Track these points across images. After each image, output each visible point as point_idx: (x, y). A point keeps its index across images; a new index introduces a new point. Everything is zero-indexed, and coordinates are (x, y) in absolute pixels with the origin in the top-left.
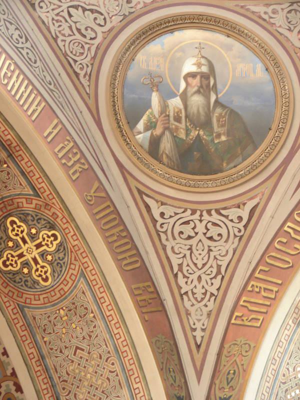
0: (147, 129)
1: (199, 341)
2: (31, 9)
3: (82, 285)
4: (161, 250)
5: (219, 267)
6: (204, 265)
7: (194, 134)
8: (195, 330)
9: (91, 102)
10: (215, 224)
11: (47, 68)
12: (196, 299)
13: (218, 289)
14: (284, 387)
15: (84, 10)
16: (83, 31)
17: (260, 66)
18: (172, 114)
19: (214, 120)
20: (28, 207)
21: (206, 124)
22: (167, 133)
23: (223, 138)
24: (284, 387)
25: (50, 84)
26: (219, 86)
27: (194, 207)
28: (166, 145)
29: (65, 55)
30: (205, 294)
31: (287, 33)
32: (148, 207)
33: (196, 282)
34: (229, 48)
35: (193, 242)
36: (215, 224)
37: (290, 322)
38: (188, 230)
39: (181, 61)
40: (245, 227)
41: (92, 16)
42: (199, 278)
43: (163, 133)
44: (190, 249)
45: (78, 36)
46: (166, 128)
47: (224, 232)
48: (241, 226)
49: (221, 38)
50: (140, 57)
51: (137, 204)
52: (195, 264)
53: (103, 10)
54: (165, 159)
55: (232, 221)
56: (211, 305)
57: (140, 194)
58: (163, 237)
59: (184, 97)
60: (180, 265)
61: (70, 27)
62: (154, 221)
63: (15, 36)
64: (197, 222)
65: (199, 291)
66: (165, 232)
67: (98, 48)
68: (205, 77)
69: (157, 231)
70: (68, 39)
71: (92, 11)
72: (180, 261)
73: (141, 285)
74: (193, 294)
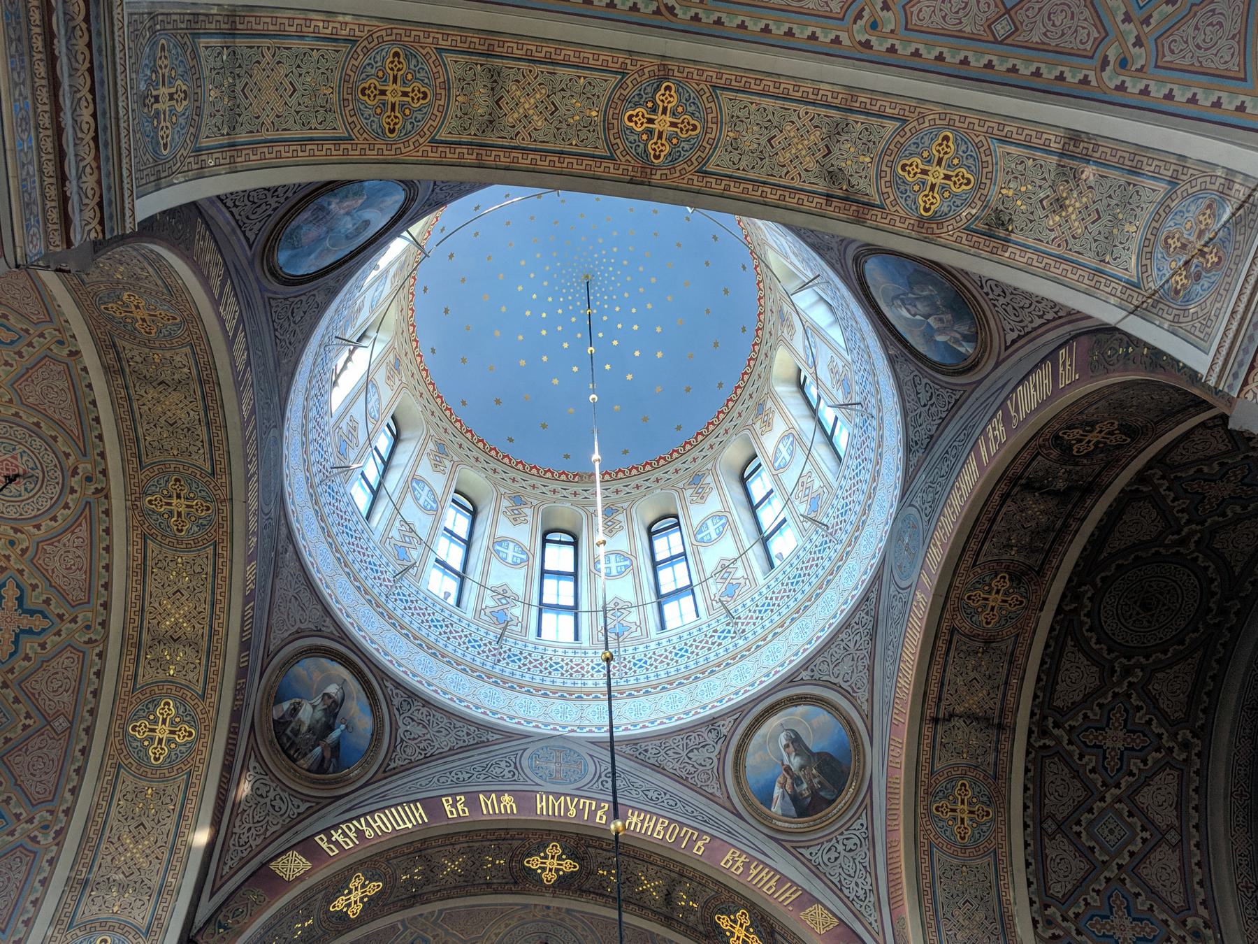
0: (961, 345)
3: (1092, 410)
14: (1071, 241)
15: (918, 393)
16: (929, 394)
24: (1071, 241)
29: (949, 411)
32: (1014, 342)
37: (1007, 255)
38: (1009, 309)
39: (906, 319)
41: (918, 387)
59: (927, 316)
61: (932, 405)
73: (1061, 369)
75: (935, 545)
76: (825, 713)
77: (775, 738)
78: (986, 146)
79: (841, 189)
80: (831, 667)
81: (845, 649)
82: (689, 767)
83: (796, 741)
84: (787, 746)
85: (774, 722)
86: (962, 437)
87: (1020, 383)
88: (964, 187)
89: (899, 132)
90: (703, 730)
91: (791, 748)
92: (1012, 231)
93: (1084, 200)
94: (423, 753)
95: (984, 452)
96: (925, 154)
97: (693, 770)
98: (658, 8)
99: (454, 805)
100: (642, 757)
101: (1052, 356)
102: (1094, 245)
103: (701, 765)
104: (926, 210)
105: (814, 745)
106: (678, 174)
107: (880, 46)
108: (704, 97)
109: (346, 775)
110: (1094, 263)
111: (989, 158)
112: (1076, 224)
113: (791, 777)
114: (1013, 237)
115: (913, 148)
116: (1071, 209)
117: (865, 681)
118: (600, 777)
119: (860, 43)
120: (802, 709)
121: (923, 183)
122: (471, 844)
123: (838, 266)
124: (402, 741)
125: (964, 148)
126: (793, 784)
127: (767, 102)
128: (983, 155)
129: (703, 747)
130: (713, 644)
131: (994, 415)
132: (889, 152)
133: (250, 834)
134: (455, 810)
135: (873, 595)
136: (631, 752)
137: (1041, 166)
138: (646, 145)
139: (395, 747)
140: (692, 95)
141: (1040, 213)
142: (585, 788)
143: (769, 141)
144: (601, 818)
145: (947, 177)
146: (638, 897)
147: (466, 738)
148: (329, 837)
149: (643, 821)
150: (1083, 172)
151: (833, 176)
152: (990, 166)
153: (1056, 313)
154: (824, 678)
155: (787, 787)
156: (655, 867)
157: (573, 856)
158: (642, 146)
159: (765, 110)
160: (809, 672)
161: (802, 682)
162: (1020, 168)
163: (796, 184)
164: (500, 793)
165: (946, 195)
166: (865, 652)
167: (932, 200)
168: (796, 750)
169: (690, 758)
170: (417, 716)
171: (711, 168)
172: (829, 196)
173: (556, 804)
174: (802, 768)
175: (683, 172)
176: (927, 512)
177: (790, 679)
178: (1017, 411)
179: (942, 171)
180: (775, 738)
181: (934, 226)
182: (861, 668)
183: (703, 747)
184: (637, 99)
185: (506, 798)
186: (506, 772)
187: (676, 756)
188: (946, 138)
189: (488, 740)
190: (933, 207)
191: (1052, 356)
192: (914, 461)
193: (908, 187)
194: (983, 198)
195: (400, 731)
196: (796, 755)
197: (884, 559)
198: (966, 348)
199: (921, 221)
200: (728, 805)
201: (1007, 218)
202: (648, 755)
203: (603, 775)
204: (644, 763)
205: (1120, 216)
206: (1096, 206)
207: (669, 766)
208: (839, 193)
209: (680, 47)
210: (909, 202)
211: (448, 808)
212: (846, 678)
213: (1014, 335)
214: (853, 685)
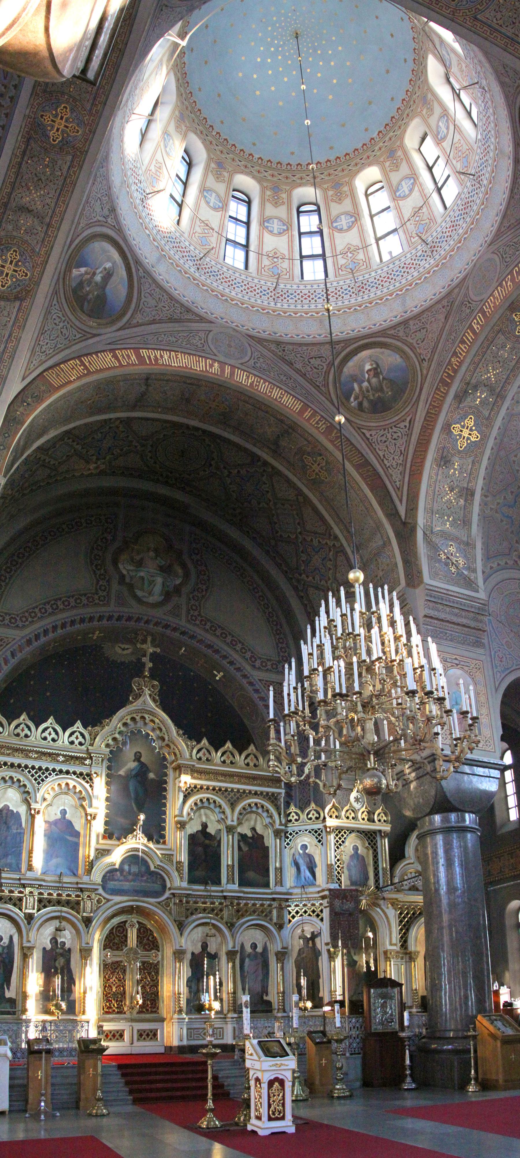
9: (328, 396)
11: (303, 387)
20: (309, 450)
34: (383, 353)
45: (315, 370)
50: (345, 370)
63: (284, 379)
75: (248, 378)
117: (147, 319)
123: (392, 332)
135: (190, 316)
156: (53, 205)
197: (211, 322)
213: (368, 436)
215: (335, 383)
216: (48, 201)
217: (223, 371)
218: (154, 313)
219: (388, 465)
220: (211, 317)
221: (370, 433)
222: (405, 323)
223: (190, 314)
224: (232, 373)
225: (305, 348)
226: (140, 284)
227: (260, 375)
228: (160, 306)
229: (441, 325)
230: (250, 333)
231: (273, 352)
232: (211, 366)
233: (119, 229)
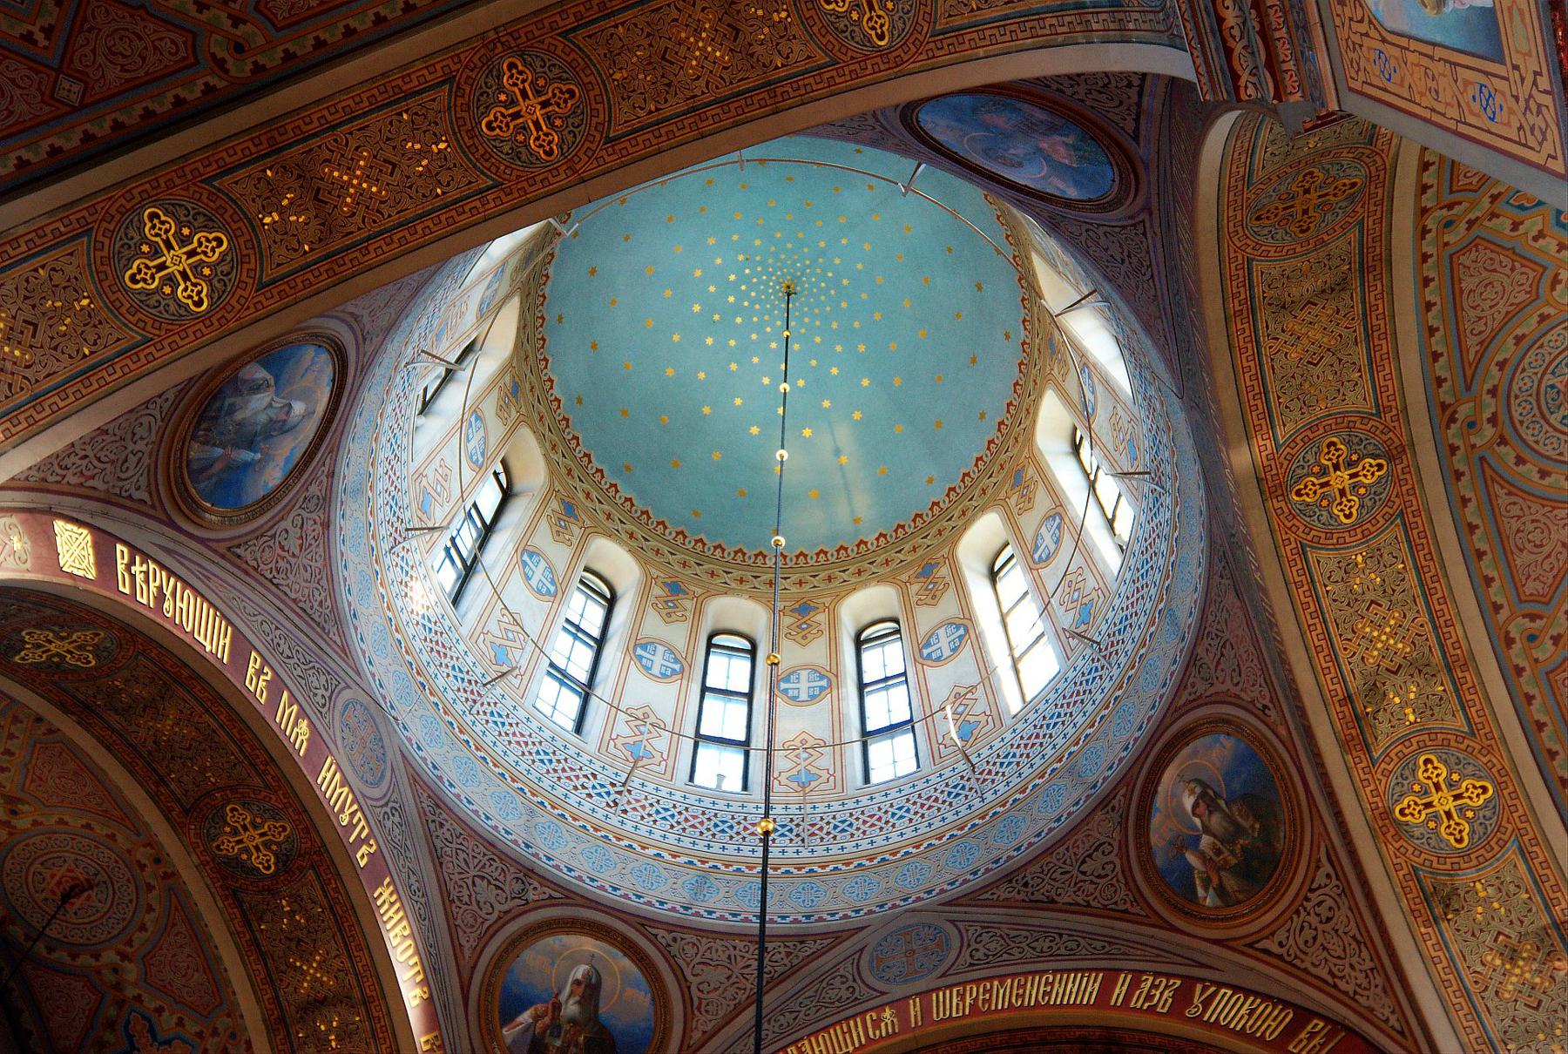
0: (1206, 889)
1: (1397, 1026)
2: (1051, 906)
4: (1306, 976)
5: (1354, 937)
6: (1344, 950)
7: (1238, 849)
8: (1387, 1021)
9: (1153, 920)
10: (1320, 904)
12: (1365, 989)
13: (1372, 960)
14: (1490, 993)
16: (1103, 873)
17: (1222, 738)
18: (1211, 854)
19: (1240, 820)
21: (1239, 831)
22: (1223, 873)
23: (1257, 826)
25: (1104, 947)
26: (1217, 789)
27: (1293, 908)
28: (1231, 883)
29: (1105, 907)
30: (1367, 976)
31: (1213, 690)
32: (1266, 951)
33: (1353, 974)
35: (1320, 939)
36: (1320, 904)
37: (1423, 930)
38: (1308, 933)
39: (1181, 806)
40: (1338, 879)
42: (1352, 966)
43: (1220, 878)
44: (1324, 949)
46: (1218, 870)
47: (1330, 902)
48: (1334, 882)
49: (1186, 751)
50: (1154, 839)
51: (1257, 959)
52: (1339, 957)
53: (1103, 839)
54: (1241, 897)
55: (1326, 885)
56: (1379, 980)
57: (1250, 946)
58: (1296, 962)
59: (1207, 830)
60: (1331, 972)
62: (1280, 957)
64: (1308, 918)
65: (1361, 979)
66: (1296, 957)
67: (1123, 872)
68: (1203, 795)
69: (1289, 963)
70: (1097, 894)
71: (1096, 850)
72: (1327, 970)
73: (1303, 1035)
74: (1360, 986)
75: (962, 996)
76: (649, 995)
77: (574, 961)
78: (1505, 837)
79: (1365, 708)
80: (698, 959)
81: (729, 957)
82: (465, 892)
83: (590, 990)
84: (577, 983)
85: (588, 944)
86: (1099, 945)
87: (1236, 989)
88: (1452, 839)
89: (1460, 737)
90: (512, 870)
91: (581, 989)
92: (1449, 920)
93: (1537, 980)
94: (274, 572)
95: (1120, 991)
96: (1455, 777)
97: (466, 899)
98: (1450, 405)
99: (259, 672)
100: (432, 826)
101: (1303, 1015)
102: (1508, 1022)
103: (478, 902)
104: (1402, 812)
105: (606, 1008)
106: (1289, 525)
107: (1517, 655)
108: (1387, 509)
109: (205, 510)
110: (1496, 1037)
111: (1497, 848)
112: (1510, 987)
113: (553, 1019)
114: (1444, 925)
115: (1453, 760)
116: (1517, 971)
117: (721, 1013)
118: (387, 804)
119: (1508, 633)
120: (626, 963)
121: (1426, 793)
122: (221, 732)
124: (273, 536)
125: (1488, 814)
126: (547, 1027)
127: (1412, 576)
128: (1495, 840)
129: (497, 887)
130: (584, 787)
131: (1168, 976)
132: (1433, 736)
133: (79, 462)
134: (256, 683)
135: (811, 947)
136: (427, 809)
137: (1530, 911)
138: (1308, 475)
139: (262, 536)
140: (1383, 496)
141: (1488, 939)
142: (369, 802)
143: (1372, 602)
144: (363, 856)
145: (1448, 814)
146: (283, 968)
147: (316, 605)
148: (132, 562)
149: (392, 904)
150: (1559, 960)
151: (1374, 690)
152: (1491, 854)
153: (1355, 993)
154: (681, 962)
155: (540, 1024)
156: (348, 964)
157: (284, 859)
158: (1305, 471)
159: (1403, 580)
160: (669, 937)
161: (652, 938)
162: (1512, 888)
163: (1342, 655)
164: (302, 714)
165: (1432, 825)
166: (749, 986)
167: (1416, 813)
168: (583, 997)
169: (474, 884)
170: (309, 526)
171: (1312, 557)
172: (1349, 698)
173: (338, 791)
174: (572, 1021)
175: (1294, 529)
176: (977, 955)
177: (644, 923)
178: (1206, 1003)
179: (1451, 805)
180: (574, 961)
181: (1392, 831)
182: (728, 994)
183: (497, 887)
184: (1356, 440)
185: (304, 724)
186: (320, 692)
187: (463, 865)
188: (1485, 789)
189: (328, 634)
190: (1409, 818)
191: (1303, 1015)
192: (1003, 892)
193: (1411, 779)
194: (1456, 866)
195: (283, 525)
196: (579, 1002)
197: (863, 928)
198: (1209, 899)
199: (1387, 814)
200: (466, 975)
201: (1456, 907)
202: (440, 832)
203: (391, 804)
204: (429, 836)
205: (1558, 1032)
206: (1543, 997)
207: (448, 868)
208: (1360, 708)
209: (1428, 459)
210: (1398, 789)
211: (251, 671)
212: (704, 987)
214: (704, 1002)
215: (1148, 880)
216: (337, 964)
217: (902, 1015)
218: (732, 990)
219: (1350, 988)
220: (856, 920)
221: (1277, 939)
222: (1192, 661)
223: (810, 944)
224: (926, 1010)
225: (1062, 850)
226: (669, 958)
227: (992, 972)
228: (737, 971)
229: (1240, 614)
230: (946, 897)
231: (1006, 904)
232: (876, 1024)
233: (569, 895)
